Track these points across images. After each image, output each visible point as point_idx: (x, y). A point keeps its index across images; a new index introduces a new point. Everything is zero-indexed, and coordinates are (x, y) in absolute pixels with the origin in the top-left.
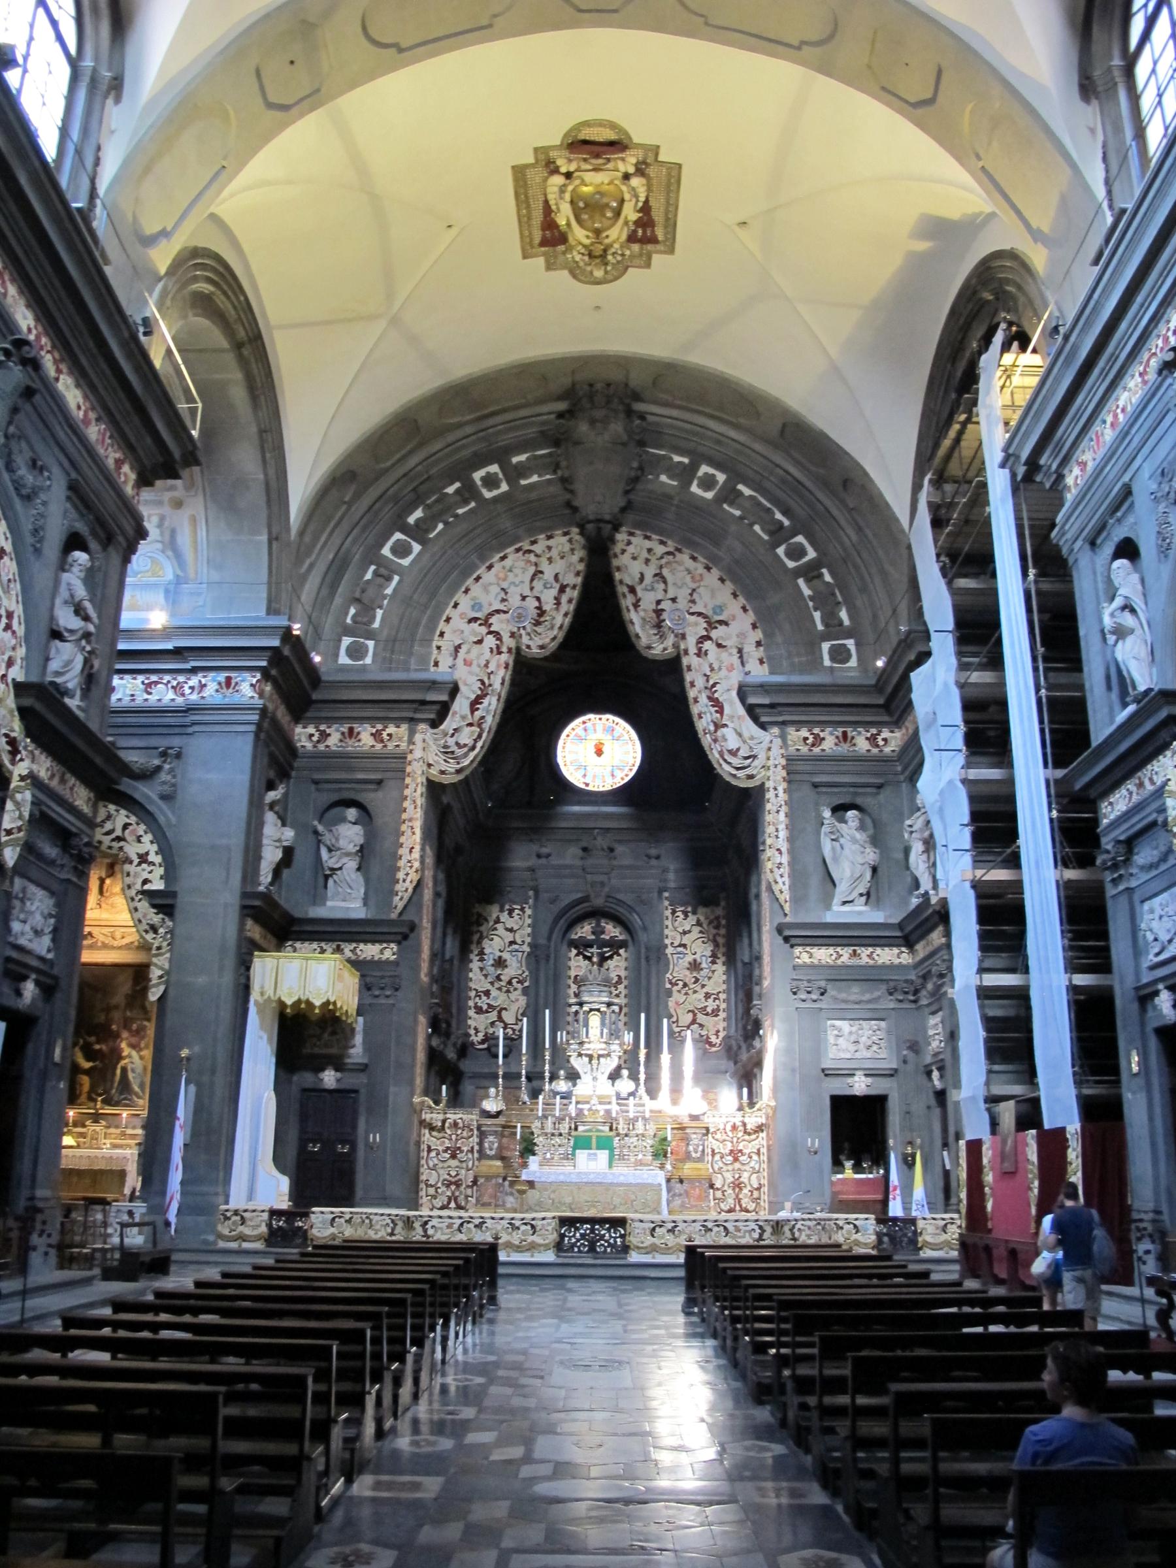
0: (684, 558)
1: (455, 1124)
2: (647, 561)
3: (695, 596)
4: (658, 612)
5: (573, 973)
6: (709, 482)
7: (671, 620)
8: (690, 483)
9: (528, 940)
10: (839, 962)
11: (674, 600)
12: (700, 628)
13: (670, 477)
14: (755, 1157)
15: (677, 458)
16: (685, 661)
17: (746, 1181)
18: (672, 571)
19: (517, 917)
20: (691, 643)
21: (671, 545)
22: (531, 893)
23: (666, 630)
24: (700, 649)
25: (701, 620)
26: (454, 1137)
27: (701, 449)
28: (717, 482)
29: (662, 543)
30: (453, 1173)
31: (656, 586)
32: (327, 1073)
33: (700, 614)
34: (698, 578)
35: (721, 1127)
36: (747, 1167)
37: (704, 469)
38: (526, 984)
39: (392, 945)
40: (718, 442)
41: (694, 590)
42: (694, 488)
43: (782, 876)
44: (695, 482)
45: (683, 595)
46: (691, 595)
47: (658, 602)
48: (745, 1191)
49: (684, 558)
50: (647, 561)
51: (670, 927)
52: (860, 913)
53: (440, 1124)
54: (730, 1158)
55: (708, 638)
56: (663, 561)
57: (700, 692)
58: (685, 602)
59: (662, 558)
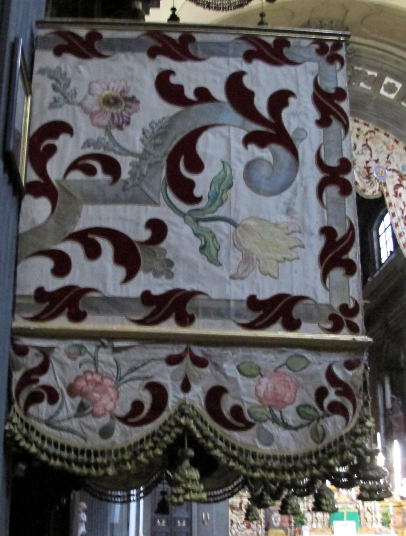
0: (381, 134)
2: (358, 136)
3: (390, 158)
4: (368, 169)
6: (391, 89)
7: (377, 174)
8: (380, 88)
11: (377, 161)
12: (396, 179)
13: (367, 84)
15: (370, 73)
16: (387, 200)
18: (375, 143)
20: (390, 188)
21: (372, 127)
23: (374, 179)
24: (396, 193)
25: (395, 174)
27: (385, 67)
28: (397, 88)
29: (365, 124)
31: (364, 151)
33: (394, 170)
34: (391, 147)
37: (388, 80)
40: (398, 63)
41: (388, 155)
42: (382, 92)
44: (382, 88)
45: (382, 158)
46: (388, 158)
47: (367, 162)
49: (381, 134)
50: (358, 136)
53: (238, 506)
55: (401, 185)
56: (368, 136)
57: (399, 219)
58: (384, 162)
59: (367, 134)
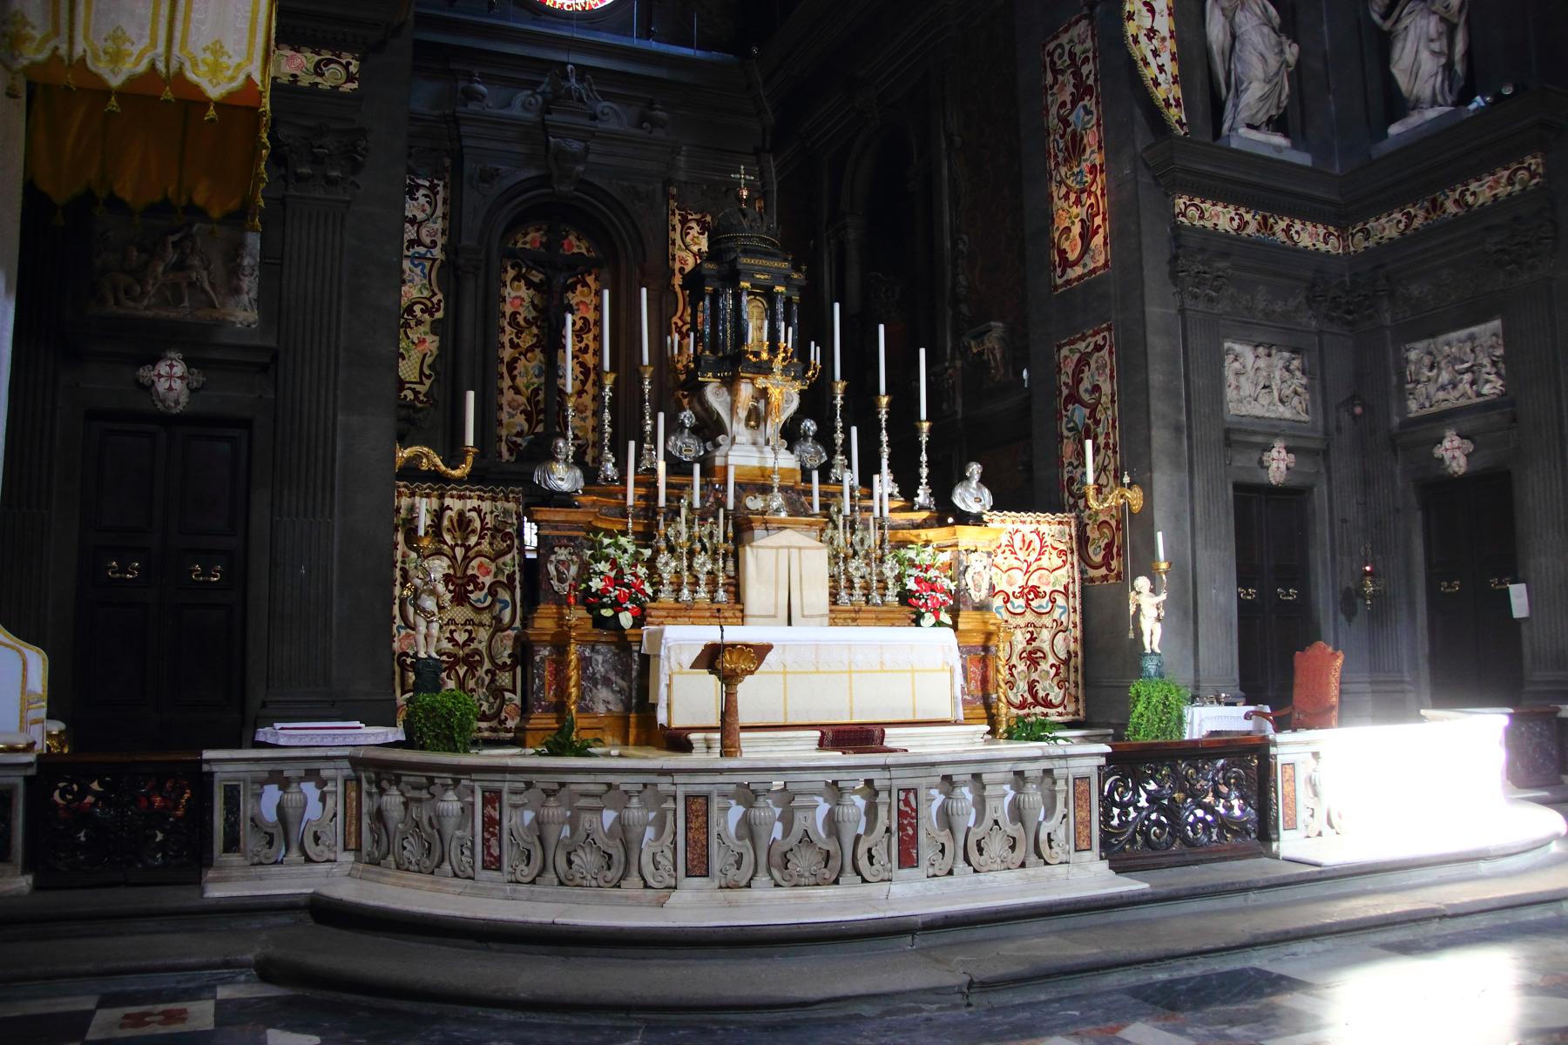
1: (462, 522)
5: (508, 309)
9: (441, 241)
10: (1287, 221)
14: (1060, 600)
17: (1046, 647)
19: (422, 200)
22: (447, 162)
26: (459, 552)
30: (461, 637)
32: (163, 368)
35: (1004, 540)
36: (1047, 620)
38: (439, 315)
39: (346, 58)
43: (1155, 53)
48: (1044, 666)
51: (678, 241)
52: (1278, 148)
54: (1021, 602)
